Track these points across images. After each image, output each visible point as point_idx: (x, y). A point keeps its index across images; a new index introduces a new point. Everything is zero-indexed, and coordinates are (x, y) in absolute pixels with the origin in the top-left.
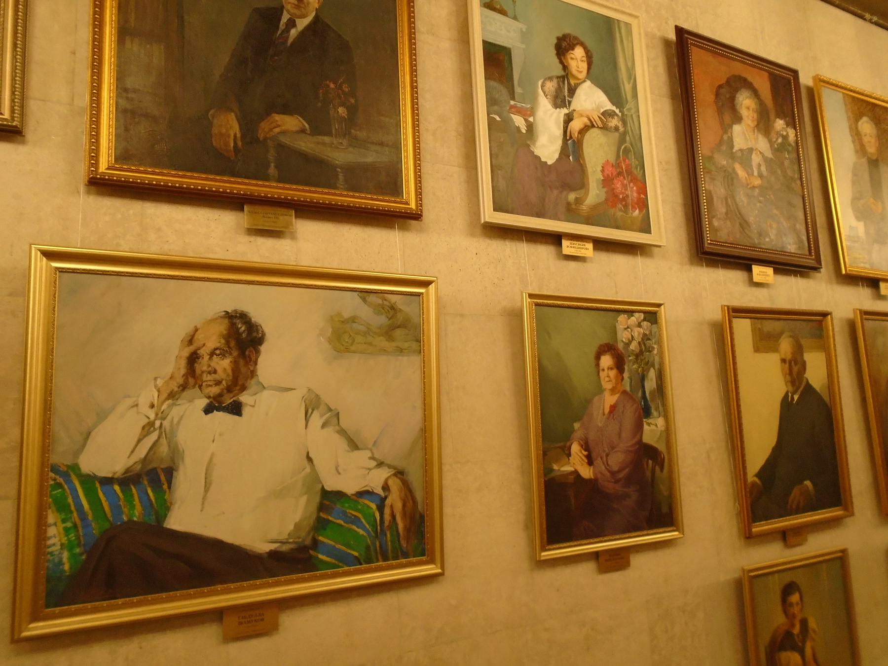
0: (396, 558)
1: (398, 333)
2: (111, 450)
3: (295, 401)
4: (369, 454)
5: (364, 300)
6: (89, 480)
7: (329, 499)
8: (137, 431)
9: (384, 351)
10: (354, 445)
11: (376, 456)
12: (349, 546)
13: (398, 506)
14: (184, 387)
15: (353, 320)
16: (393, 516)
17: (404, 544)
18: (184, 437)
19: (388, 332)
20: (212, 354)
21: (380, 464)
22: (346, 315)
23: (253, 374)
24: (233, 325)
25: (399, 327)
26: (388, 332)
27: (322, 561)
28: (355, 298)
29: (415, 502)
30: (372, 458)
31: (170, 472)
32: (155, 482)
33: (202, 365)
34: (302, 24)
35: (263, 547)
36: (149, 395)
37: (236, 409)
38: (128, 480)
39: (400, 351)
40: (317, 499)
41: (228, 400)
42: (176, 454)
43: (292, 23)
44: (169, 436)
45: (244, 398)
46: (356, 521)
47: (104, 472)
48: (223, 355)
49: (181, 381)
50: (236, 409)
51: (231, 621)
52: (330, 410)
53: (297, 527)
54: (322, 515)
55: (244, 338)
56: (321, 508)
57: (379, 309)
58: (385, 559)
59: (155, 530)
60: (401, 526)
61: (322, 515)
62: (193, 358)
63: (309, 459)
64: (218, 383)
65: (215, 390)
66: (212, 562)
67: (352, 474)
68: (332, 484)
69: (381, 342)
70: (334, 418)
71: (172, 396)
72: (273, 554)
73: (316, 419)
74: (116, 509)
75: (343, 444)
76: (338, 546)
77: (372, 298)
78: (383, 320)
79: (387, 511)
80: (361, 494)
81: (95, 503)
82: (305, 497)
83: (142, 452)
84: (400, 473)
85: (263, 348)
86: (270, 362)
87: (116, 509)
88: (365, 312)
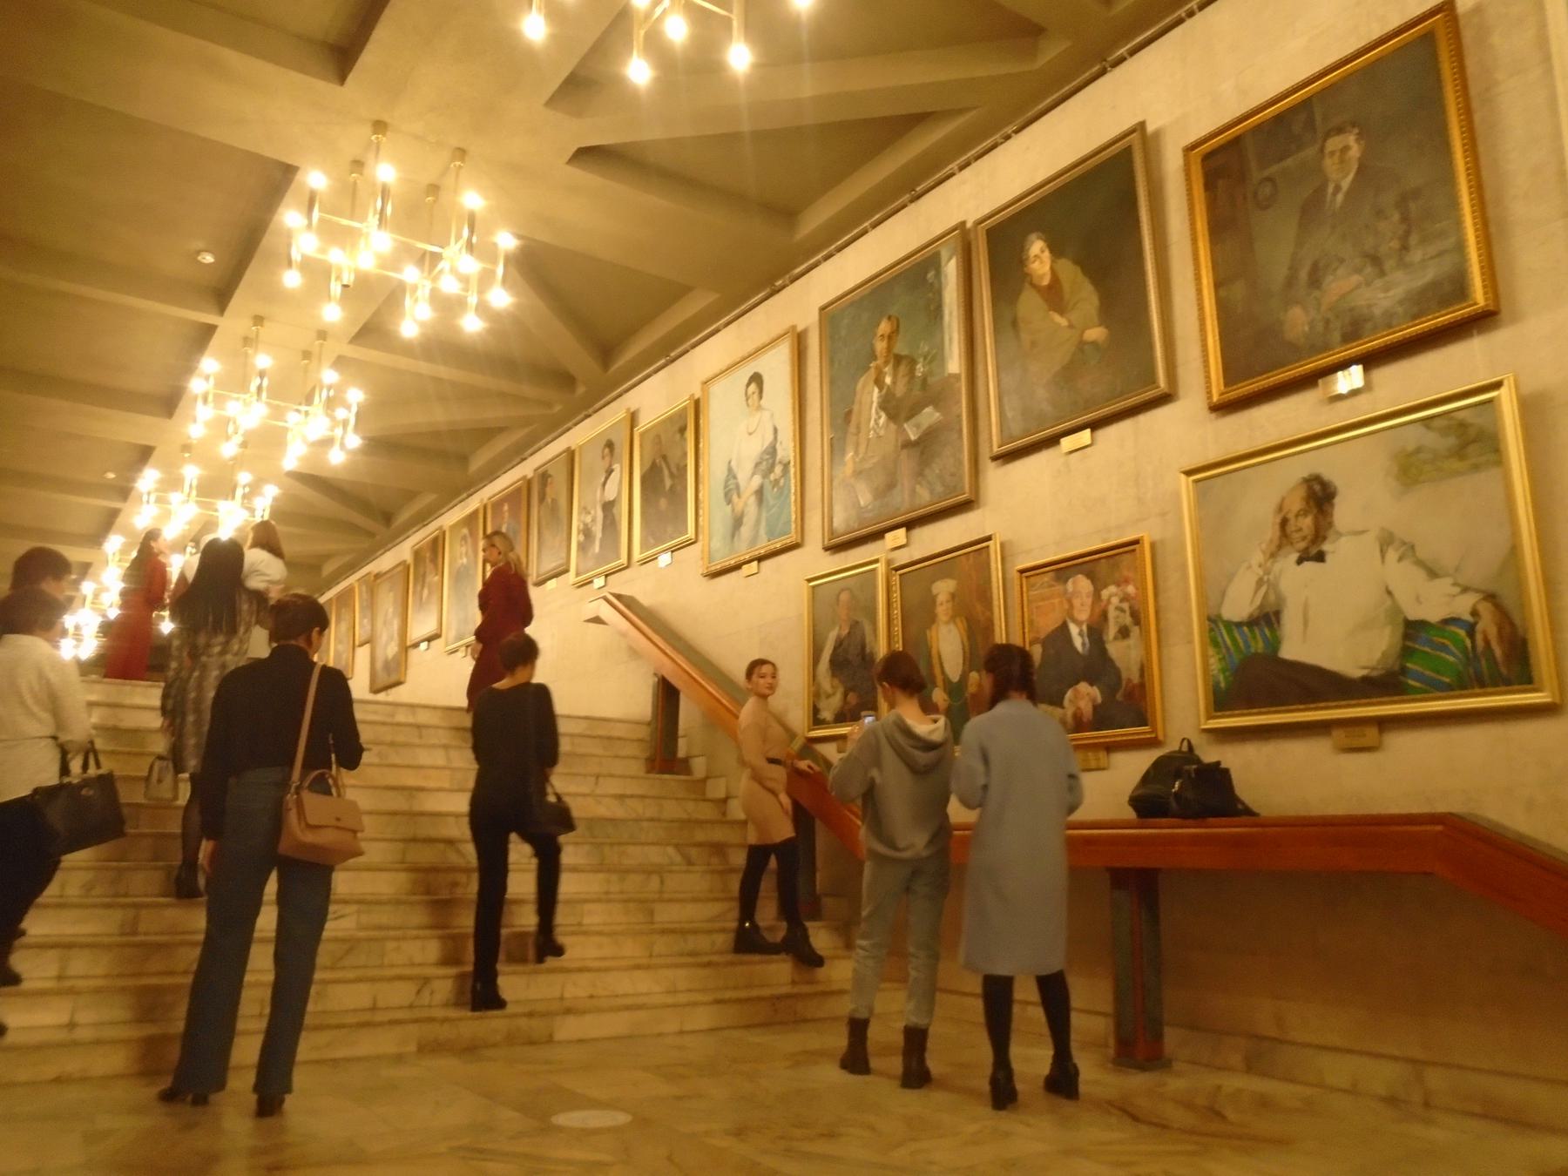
0: (1496, 685)
1: (1471, 449)
2: (1239, 604)
3: (1370, 542)
4: (1449, 581)
5: (1428, 427)
6: (1229, 625)
7: (1413, 629)
8: (1253, 585)
9: (1457, 473)
10: (1433, 574)
11: (1460, 581)
12: (1438, 672)
13: (1493, 632)
14: (1280, 547)
15: (1418, 450)
16: (1487, 642)
17: (1504, 670)
18: (1285, 586)
19: (1460, 452)
20: (1297, 516)
21: (1465, 590)
22: (1411, 447)
23: (1331, 524)
24: (1310, 488)
25: (1474, 441)
26: (1460, 452)
27: (1413, 687)
28: (1419, 428)
29: (1512, 624)
30: (1455, 584)
31: (1278, 614)
32: (1269, 624)
33: (1291, 527)
34: (1346, 184)
35: (1357, 673)
36: (1258, 557)
37: (1320, 557)
38: (1252, 622)
39: (1476, 468)
40: (1400, 630)
41: (1314, 551)
42: (1280, 600)
43: (1338, 189)
44: (1273, 586)
45: (1326, 547)
46: (1444, 648)
47: (1236, 619)
48: (1305, 515)
49: (1276, 542)
50: (1320, 557)
51: (1338, 734)
52: (1404, 543)
53: (1384, 654)
54: (1409, 644)
55: (1320, 496)
56: (1406, 636)
57: (1445, 432)
58: (1482, 685)
59: (1271, 657)
60: (1498, 652)
61: (1409, 644)
62: (1284, 523)
63: (1389, 593)
64: (1304, 538)
65: (1302, 545)
66: (1317, 684)
67: (1435, 602)
68: (1414, 614)
69: (1456, 465)
70: (1409, 551)
71: (1273, 555)
72: (1366, 680)
73: (1392, 555)
74: (1246, 642)
75: (1420, 574)
76: (1427, 673)
77: (1437, 423)
78: (1451, 441)
79: (1479, 638)
80: (1447, 621)
81: (1234, 640)
82: (1387, 631)
83: (1258, 602)
84: (1491, 597)
85: (1337, 500)
86: (1344, 512)
87: (1248, 646)
88: (1431, 439)
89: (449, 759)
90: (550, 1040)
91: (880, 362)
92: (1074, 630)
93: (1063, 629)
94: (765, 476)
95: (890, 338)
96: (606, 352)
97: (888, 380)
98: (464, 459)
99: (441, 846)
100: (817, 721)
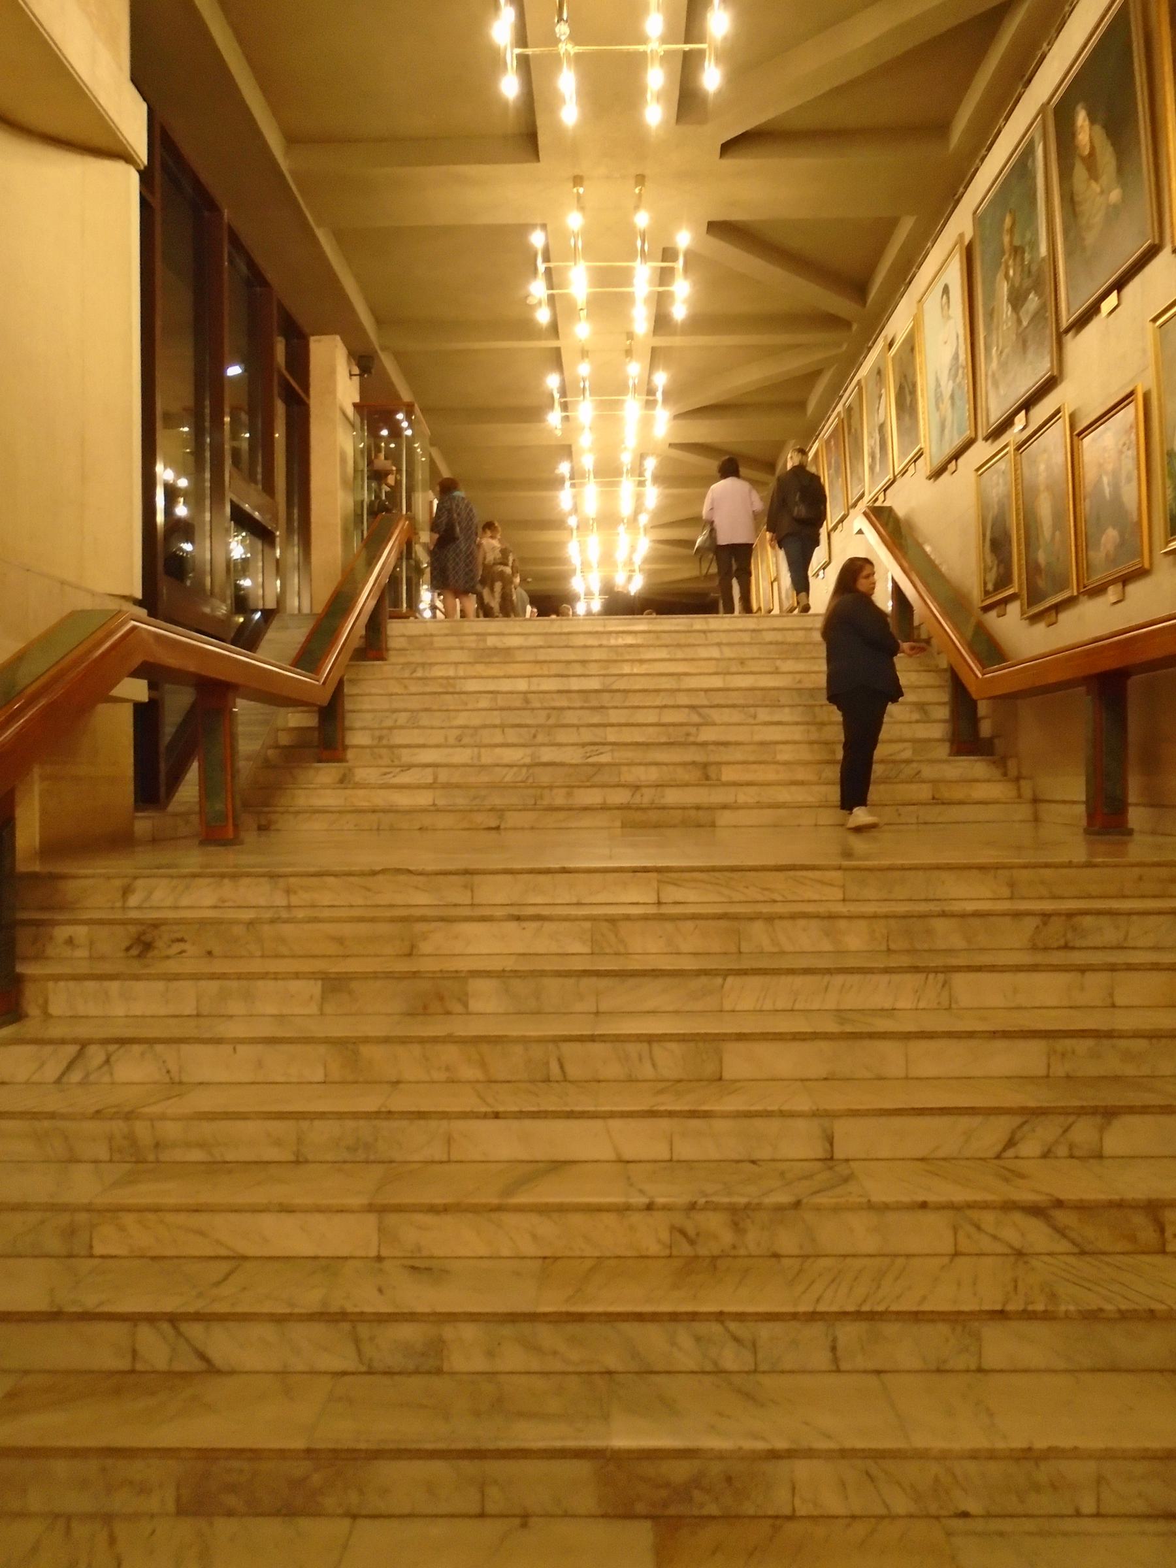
89: (722, 652)
90: (713, 825)
91: (1006, 256)
92: (1105, 480)
93: (1100, 477)
94: (954, 381)
95: (1011, 231)
96: (858, 288)
97: (1011, 272)
98: (802, 405)
99: (687, 710)
100: (987, 593)
